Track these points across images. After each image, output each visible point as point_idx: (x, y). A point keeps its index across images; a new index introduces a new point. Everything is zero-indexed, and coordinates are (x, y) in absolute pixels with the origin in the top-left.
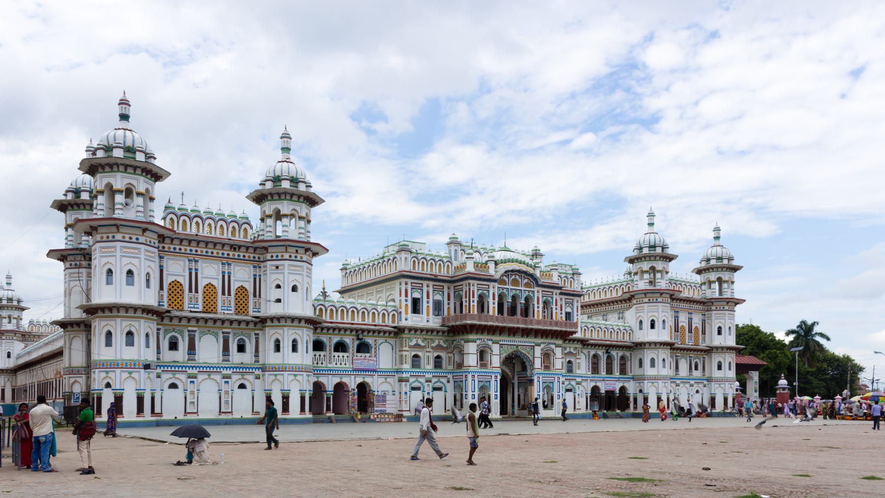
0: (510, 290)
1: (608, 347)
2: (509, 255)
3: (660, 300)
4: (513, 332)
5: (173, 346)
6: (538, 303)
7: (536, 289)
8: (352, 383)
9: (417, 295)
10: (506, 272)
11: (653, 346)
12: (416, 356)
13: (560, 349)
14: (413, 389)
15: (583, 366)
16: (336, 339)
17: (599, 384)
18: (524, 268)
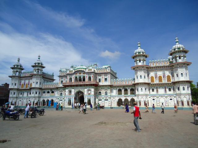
0: (78, 75)
1: (124, 87)
2: (82, 67)
3: (138, 69)
4: (77, 86)
5: (21, 94)
6: (86, 77)
7: (85, 74)
8: (50, 99)
9: (62, 80)
10: (76, 71)
11: (183, 82)
12: (61, 93)
13: (93, 89)
14: (60, 100)
15: (115, 92)
16: (47, 91)
17: (121, 98)
18: (82, 70)
